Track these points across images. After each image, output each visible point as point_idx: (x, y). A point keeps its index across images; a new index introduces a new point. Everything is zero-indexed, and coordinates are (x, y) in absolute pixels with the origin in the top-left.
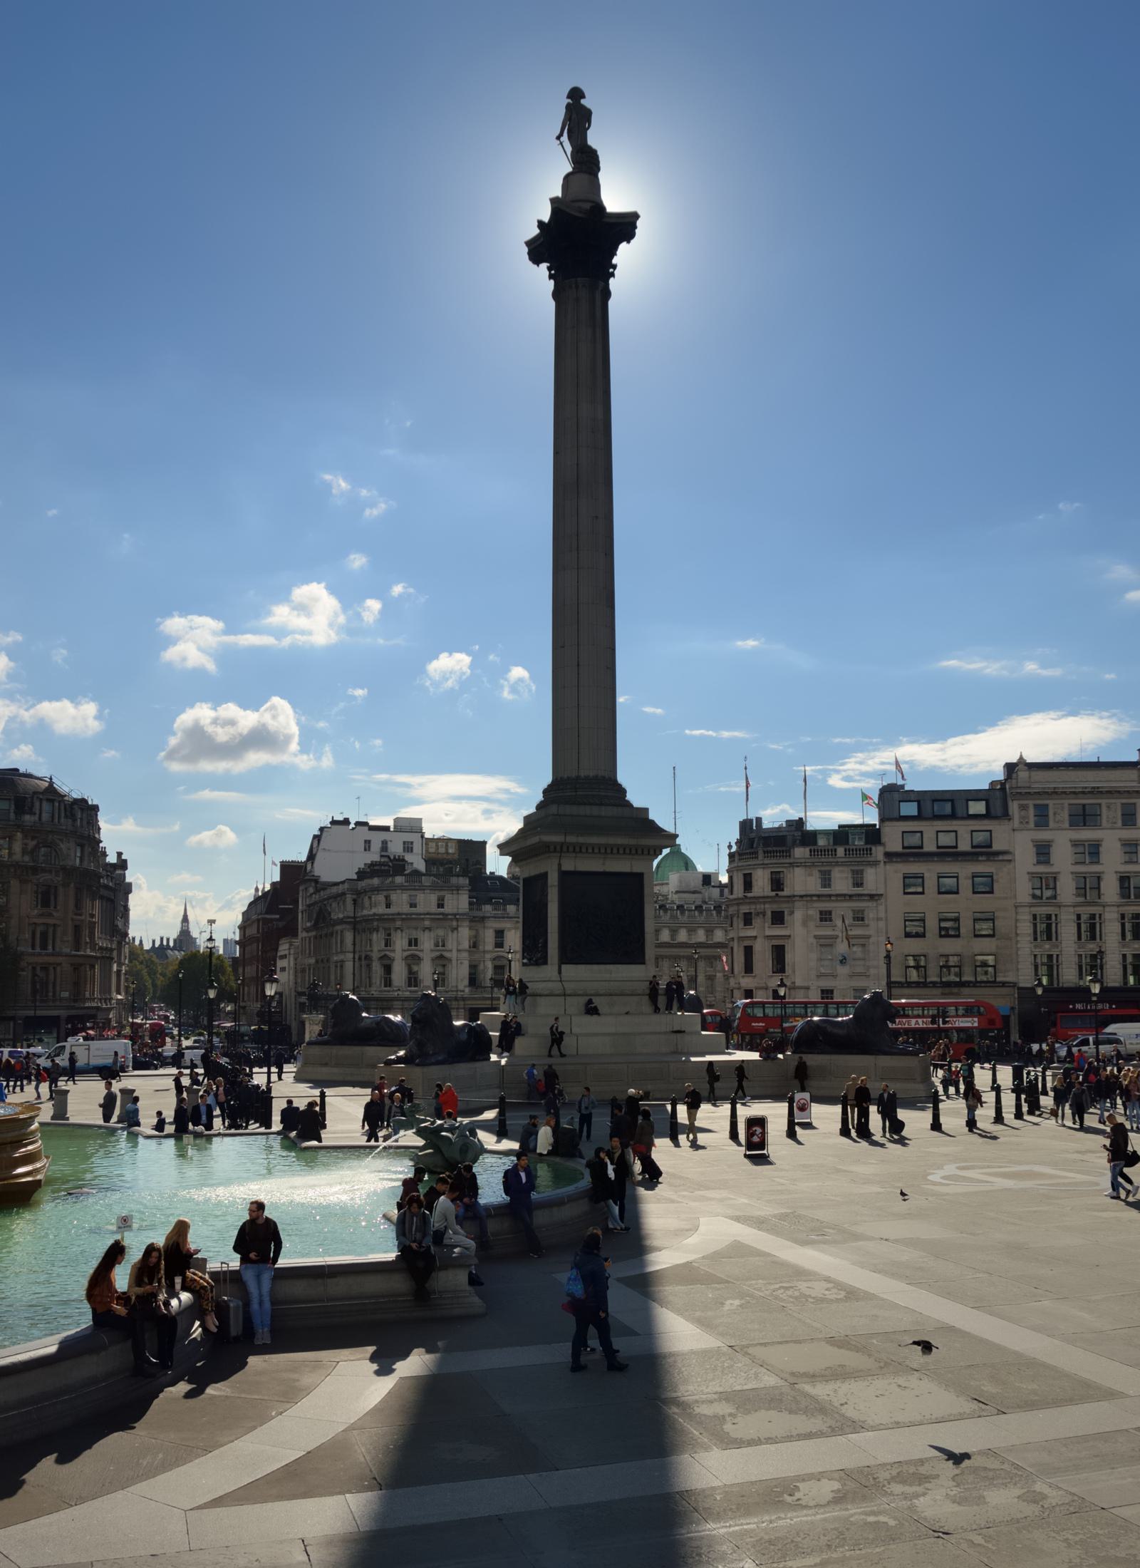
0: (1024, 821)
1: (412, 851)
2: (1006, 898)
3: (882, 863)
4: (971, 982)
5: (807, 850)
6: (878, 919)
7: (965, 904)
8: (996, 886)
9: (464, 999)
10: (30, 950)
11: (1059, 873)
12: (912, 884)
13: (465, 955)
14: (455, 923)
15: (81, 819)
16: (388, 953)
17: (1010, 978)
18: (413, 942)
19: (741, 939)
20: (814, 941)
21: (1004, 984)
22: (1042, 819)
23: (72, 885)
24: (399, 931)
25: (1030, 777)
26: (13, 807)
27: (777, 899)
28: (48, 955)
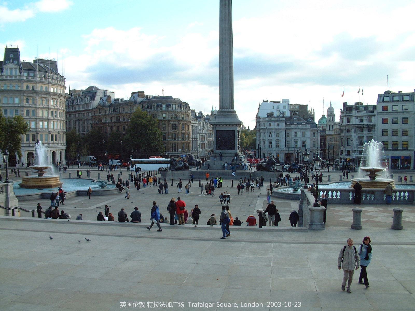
1: (286, 108)
2: (411, 125)
3: (376, 115)
5: (356, 112)
7: (400, 126)
9: (284, 151)
12: (385, 121)
13: (284, 140)
14: (281, 130)
16: (264, 139)
17: (412, 149)
18: (270, 136)
19: (341, 136)
21: (410, 150)
23: (181, 124)
24: (267, 133)
27: (349, 125)
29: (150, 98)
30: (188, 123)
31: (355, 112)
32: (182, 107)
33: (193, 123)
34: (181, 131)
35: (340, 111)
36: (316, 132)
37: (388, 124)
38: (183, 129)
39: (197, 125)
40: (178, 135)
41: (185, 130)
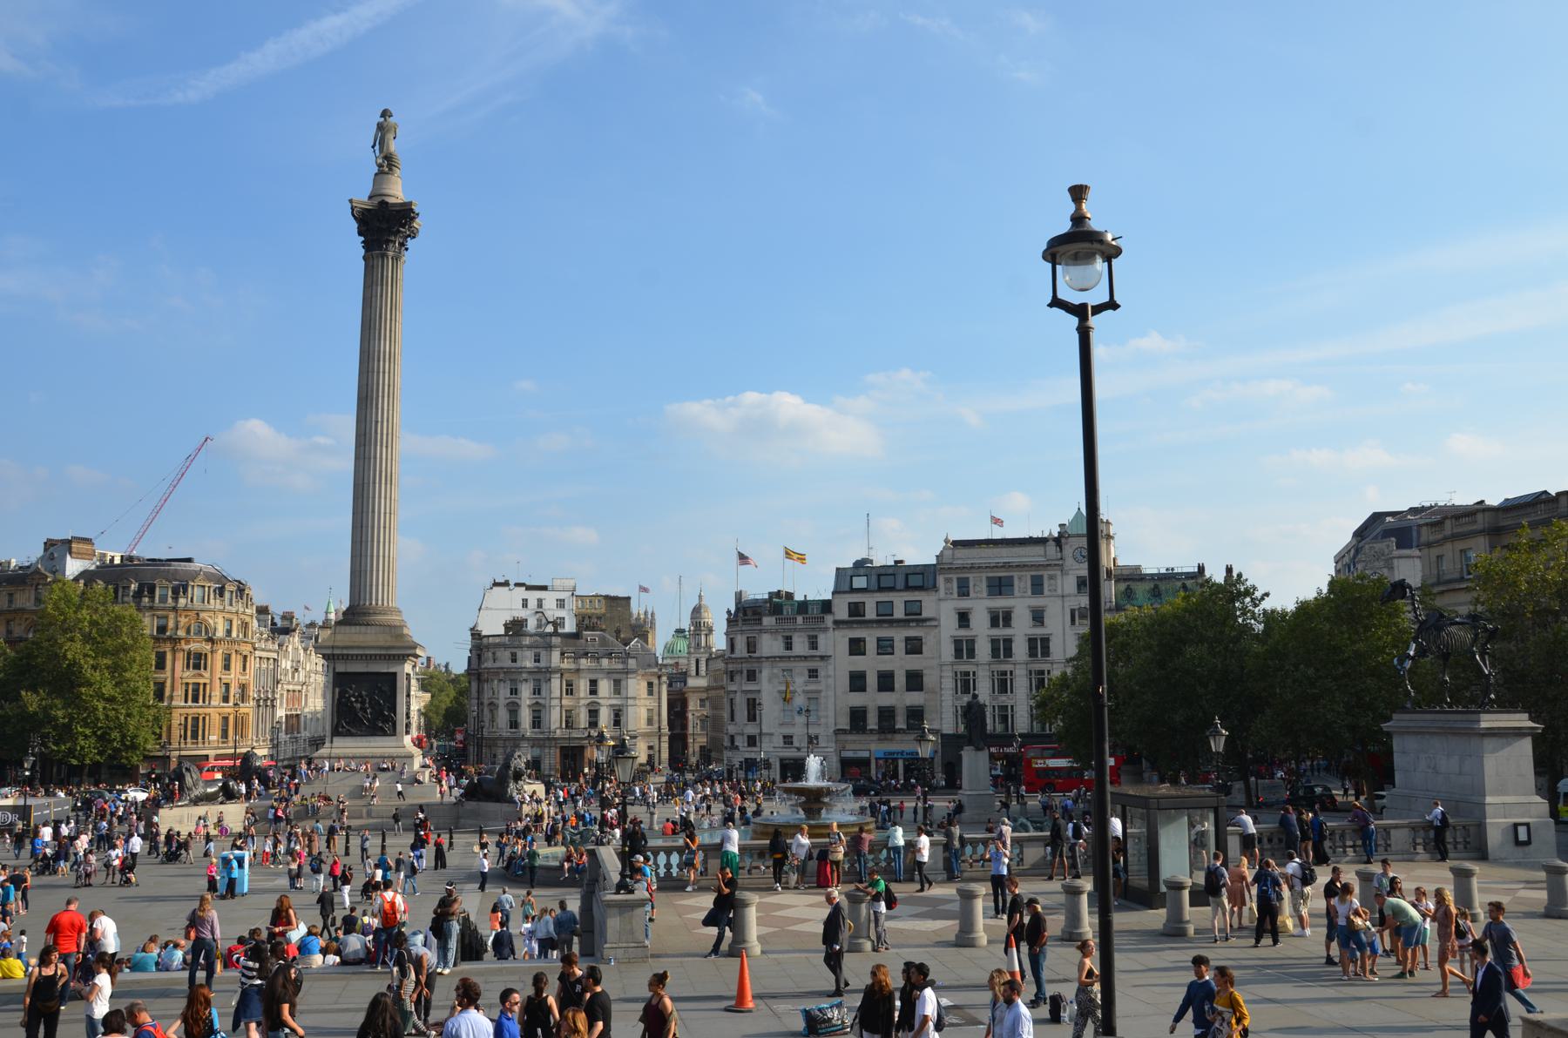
0: (948, 592)
4: (900, 729)
5: (773, 619)
6: (828, 676)
7: (899, 663)
8: (925, 648)
10: (183, 704)
11: (976, 636)
12: (857, 647)
15: (231, 600)
18: (514, 691)
19: (729, 692)
20: (778, 695)
22: (964, 591)
23: (220, 651)
25: (953, 555)
26: (170, 593)
28: (196, 707)
29: (112, 559)
30: (246, 649)
31: (768, 621)
32: (227, 595)
33: (263, 650)
34: (218, 676)
35: (726, 616)
36: (656, 681)
37: (864, 654)
38: (227, 667)
39: (275, 655)
40: (208, 687)
41: (233, 670)
